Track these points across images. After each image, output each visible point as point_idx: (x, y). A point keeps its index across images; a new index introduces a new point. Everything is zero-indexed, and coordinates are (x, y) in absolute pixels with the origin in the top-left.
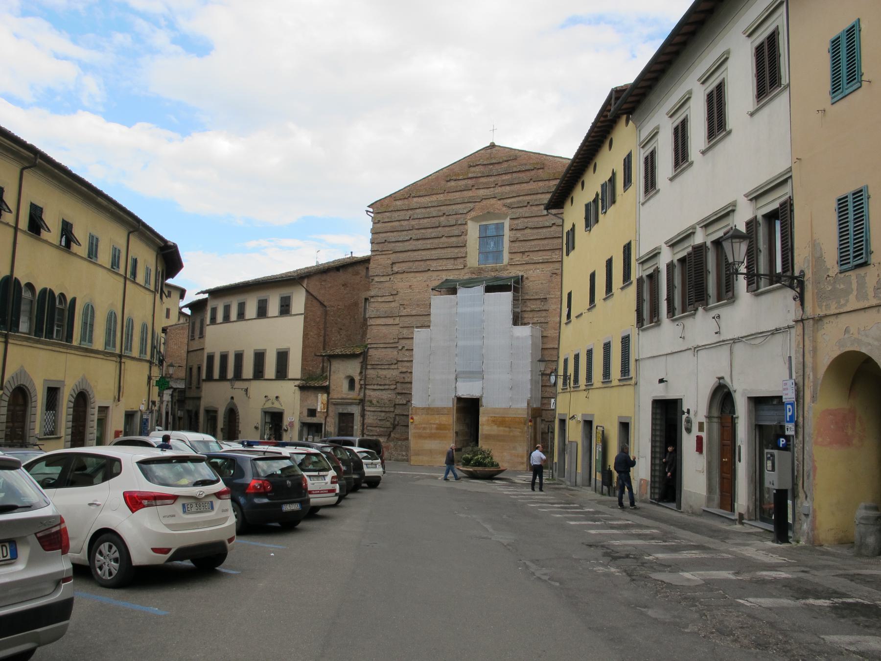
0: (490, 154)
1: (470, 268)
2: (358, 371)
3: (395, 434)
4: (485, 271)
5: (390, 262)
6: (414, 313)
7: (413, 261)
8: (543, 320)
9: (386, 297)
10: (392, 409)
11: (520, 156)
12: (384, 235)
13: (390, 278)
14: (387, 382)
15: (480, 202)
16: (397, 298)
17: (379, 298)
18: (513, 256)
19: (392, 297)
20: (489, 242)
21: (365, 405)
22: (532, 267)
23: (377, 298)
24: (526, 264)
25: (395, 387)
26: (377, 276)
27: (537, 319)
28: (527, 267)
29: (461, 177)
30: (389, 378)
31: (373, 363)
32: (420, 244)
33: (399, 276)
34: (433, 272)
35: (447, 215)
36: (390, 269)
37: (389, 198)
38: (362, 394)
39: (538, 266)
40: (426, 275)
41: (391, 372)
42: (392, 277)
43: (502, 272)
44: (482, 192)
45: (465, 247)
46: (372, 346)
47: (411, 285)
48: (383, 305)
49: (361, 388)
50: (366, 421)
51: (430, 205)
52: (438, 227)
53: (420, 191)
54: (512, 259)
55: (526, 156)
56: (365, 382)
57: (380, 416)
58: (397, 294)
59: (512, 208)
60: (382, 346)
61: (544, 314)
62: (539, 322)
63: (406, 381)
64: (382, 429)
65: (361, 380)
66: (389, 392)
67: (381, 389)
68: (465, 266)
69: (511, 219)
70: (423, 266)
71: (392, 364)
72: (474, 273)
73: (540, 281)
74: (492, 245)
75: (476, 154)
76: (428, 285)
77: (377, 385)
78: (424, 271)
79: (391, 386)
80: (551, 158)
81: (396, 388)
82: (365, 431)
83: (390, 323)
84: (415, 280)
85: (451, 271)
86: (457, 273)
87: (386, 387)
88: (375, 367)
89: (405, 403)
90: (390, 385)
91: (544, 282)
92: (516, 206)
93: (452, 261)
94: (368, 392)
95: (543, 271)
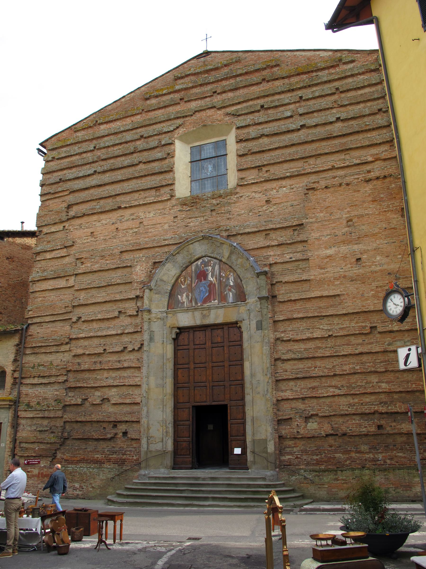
0: (204, 62)
1: (178, 199)
2: (12, 357)
3: (63, 453)
4: (203, 200)
5: (65, 205)
6: (96, 267)
7: (96, 199)
8: (299, 256)
9: (57, 252)
10: (59, 414)
11: (245, 58)
12: (60, 173)
13: (64, 227)
14: (54, 372)
15: (192, 115)
16: (72, 251)
17: (48, 253)
18: (243, 174)
19: (65, 250)
20: (205, 166)
21: (20, 408)
22: (274, 184)
23: (45, 254)
24: (266, 181)
25: (65, 378)
26: (46, 225)
27: (291, 255)
28: (268, 186)
29: (164, 92)
30: (57, 366)
31: (34, 345)
32: (107, 178)
33: (78, 222)
34: (125, 210)
35: (145, 138)
36: (64, 214)
37: (67, 131)
38: (15, 393)
39: (284, 183)
40: (115, 216)
41: (60, 356)
42: (66, 224)
43: (228, 197)
44: (193, 105)
45: (171, 173)
46: (35, 320)
47: (93, 231)
48: (52, 263)
49: (14, 384)
50: (19, 434)
51: (122, 129)
52: (132, 153)
53: (109, 116)
54: (242, 179)
55: (253, 57)
56: (21, 374)
57: (41, 425)
58: (73, 245)
59: (239, 116)
60: (48, 319)
61: (300, 247)
62: (293, 259)
63: (82, 368)
64: (43, 446)
65: (14, 371)
66: (56, 387)
67: (44, 384)
68: (172, 196)
69: (238, 128)
70: (109, 204)
71: (62, 344)
72: (185, 204)
73: (289, 204)
74: (210, 169)
75: (185, 65)
76: (117, 228)
77: (39, 377)
78: (112, 210)
79: (59, 378)
80: (289, 53)
81: (66, 381)
82: (17, 451)
83: (61, 286)
84: (98, 224)
85: (152, 205)
86: (162, 207)
87: (53, 380)
88: (37, 350)
89: (80, 403)
90: (57, 376)
91: (295, 203)
92: (243, 112)
93: (153, 192)
94: (24, 390)
95: (293, 188)
